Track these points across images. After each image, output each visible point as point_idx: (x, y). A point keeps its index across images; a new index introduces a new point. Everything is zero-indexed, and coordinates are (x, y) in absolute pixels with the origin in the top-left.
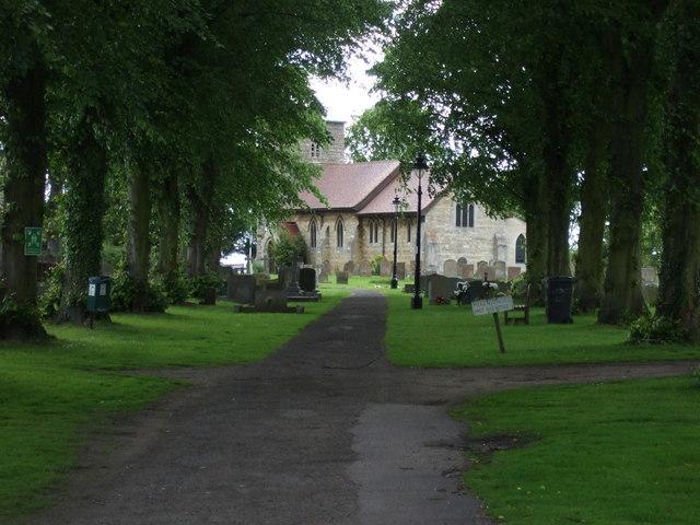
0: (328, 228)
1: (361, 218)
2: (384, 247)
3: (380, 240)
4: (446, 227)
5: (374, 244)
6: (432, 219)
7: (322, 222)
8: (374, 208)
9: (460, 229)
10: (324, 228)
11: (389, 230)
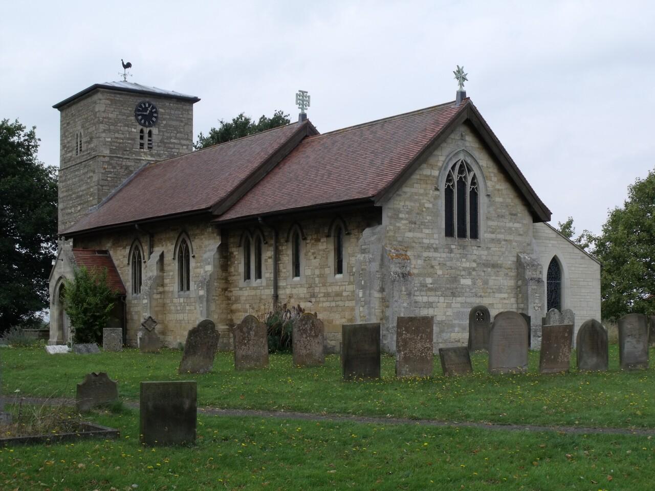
0: (162, 256)
2: (276, 287)
3: (268, 273)
5: (254, 282)
6: (396, 217)
7: (152, 247)
9: (454, 243)
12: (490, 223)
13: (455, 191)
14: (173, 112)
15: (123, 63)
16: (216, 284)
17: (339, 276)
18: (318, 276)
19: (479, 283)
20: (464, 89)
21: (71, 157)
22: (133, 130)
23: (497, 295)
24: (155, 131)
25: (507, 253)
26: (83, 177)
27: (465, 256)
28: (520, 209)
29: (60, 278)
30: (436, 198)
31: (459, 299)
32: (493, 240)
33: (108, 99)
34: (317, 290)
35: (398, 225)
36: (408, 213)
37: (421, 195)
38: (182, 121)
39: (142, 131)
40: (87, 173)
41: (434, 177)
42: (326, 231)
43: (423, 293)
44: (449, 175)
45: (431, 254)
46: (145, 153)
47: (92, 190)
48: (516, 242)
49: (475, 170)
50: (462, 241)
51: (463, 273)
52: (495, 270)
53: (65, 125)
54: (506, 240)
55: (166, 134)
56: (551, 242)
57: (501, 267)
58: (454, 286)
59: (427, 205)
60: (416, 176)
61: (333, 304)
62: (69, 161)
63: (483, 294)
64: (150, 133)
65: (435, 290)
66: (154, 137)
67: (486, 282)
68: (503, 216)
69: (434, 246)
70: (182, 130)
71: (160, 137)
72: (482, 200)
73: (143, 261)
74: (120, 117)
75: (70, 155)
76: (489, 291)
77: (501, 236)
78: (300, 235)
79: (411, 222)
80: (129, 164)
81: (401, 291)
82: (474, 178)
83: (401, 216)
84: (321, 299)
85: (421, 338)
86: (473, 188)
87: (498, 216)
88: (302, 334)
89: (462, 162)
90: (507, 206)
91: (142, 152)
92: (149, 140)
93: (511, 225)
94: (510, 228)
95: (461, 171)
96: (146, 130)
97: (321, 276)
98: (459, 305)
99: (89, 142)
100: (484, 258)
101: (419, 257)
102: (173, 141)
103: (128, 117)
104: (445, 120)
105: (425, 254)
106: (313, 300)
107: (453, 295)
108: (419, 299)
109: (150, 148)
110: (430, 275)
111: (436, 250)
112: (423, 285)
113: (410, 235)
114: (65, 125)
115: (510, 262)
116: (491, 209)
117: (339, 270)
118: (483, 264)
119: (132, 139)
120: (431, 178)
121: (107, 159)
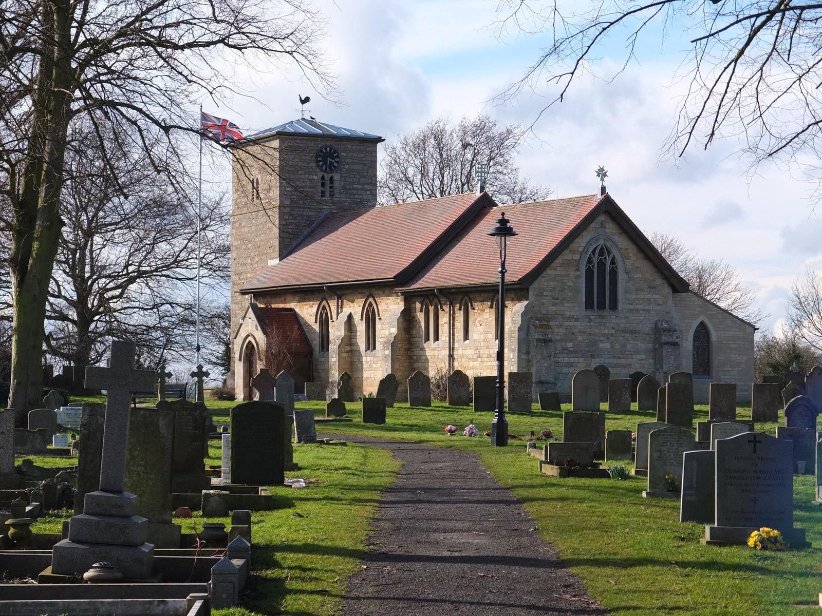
0: (350, 317)
4: (568, 309)
7: (340, 308)
8: (432, 279)
9: (593, 315)
10: (343, 317)
11: (460, 316)
12: (630, 296)
14: (355, 155)
15: (300, 98)
19: (617, 346)
28: (659, 281)
29: (248, 336)
30: (577, 277)
35: (543, 301)
38: (365, 165)
39: (323, 178)
41: (575, 260)
42: (489, 303)
44: (590, 258)
45: (571, 324)
49: (615, 252)
50: (600, 313)
51: (602, 338)
54: (644, 310)
55: (348, 179)
59: (568, 284)
63: (621, 356)
64: (332, 179)
65: (576, 352)
66: (336, 184)
68: (641, 290)
69: (575, 317)
70: (365, 174)
71: (342, 183)
72: (621, 277)
77: (641, 307)
79: (554, 298)
82: (613, 259)
89: (602, 246)
90: (646, 281)
92: (331, 187)
94: (649, 300)
95: (601, 253)
97: (485, 340)
99: (269, 190)
100: (623, 325)
101: (561, 326)
102: (355, 186)
105: (567, 324)
106: (479, 360)
107: (593, 356)
108: (560, 360)
109: (332, 196)
111: (577, 320)
112: (565, 349)
113: (554, 308)
115: (647, 329)
118: (622, 331)
121: (288, 210)
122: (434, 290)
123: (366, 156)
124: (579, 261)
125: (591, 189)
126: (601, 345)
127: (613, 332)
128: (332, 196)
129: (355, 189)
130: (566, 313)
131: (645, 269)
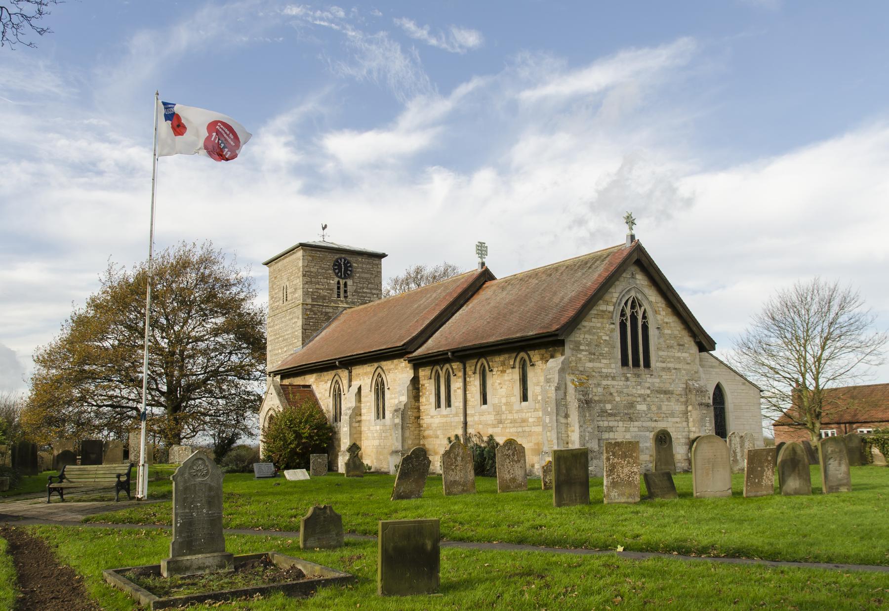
0: (360, 389)
1: (418, 364)
6: (577, 349)
10: (354, 389)
12: (661, 353)
13: (629, 324)
14: (364, 266)
16: (409, 413)
17: (524, 404)
18: (505, 404)
19: (654, 408)
20: (633, 232)
21: (278, 306)
22: (331, 282)
23: (670, 419)
24: (350, 282)
25: (677, 380)
26: (289, 322)
27: (640, 384)
30: (612, 331)
31: (636, 424)
32: (664, 368)
33: (310, 256)
34: (504, 417)
35: (579, 356)
36: (588, 345)
37: (599, 328)
38: (372, 274)
39: (339, 283)
40: (292, 319)
41: (609, 312)
42: (512, 363)
43: (604, 418)
44: (623, 310)
45: (609, 382)
46: (342, 301)
47: (296, 333)
48: (684, 370)
49: (646, 305)
50: (636, 370)
51: (639, 399)
52: (668, 396)
53: (273, 279)
54: (676, 369)
56: (715, 370)
57: (672, 394)
58: (631, 411)
59: (604, 338)
60: (593, 312)
61: (520, 430)
62: (277, 309)
63: (657, 419)
64: (345, 285)
66: (349, 288)
67: (659, 408)
68: (672, 347)
69: (613, 375)
71: (355, 288)
72: (652, 332)
73: (342, 394)
74: (320, 270)
75: (278, 304)
76: (663, 415)
77: (671, 365)
78: (528, 362)
79: (590, 353)
80: (328, 310)
81: (585, 416)
83: (582, 347)
84: (508, 425)
85: (629, 462)
86: (644, 322)
87: (668, 347)
88: (505, 459)
89: (634, 298)
91: (339, 301)
93: (679, 354)
94: (679, 358)
95: (633, 307)
96: (342, 282)
97: (507, 404)
98: (636, 429)
99: (294, 293)
100: (657, 385)
101: (599, 385)
103: (327, 270)
104: (619, 260)
105: (604, 382)
106: (501, 426)
107: (631, 419)
109: (346, 297)
110: (609, 402)
111: (613, 378)
114: (273, 279)
115: (680, 389)
116: (661, 340)
117: (525, 398)
118: (657, 391)
119: (331, 290)
120: (606, 313)
121: (309, 307)
122: (447, 354)
123: (373, 268)
124: (612, 313)
125: (618, 238)
126: (639, 407)
127: (648, 392)
128: (346, 297)
129: (364, 293)
130: (603, 370)
131: (674, 327)
